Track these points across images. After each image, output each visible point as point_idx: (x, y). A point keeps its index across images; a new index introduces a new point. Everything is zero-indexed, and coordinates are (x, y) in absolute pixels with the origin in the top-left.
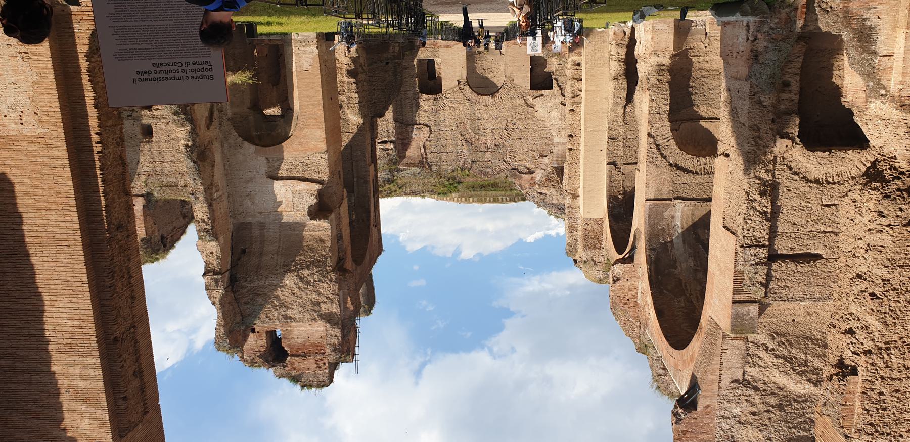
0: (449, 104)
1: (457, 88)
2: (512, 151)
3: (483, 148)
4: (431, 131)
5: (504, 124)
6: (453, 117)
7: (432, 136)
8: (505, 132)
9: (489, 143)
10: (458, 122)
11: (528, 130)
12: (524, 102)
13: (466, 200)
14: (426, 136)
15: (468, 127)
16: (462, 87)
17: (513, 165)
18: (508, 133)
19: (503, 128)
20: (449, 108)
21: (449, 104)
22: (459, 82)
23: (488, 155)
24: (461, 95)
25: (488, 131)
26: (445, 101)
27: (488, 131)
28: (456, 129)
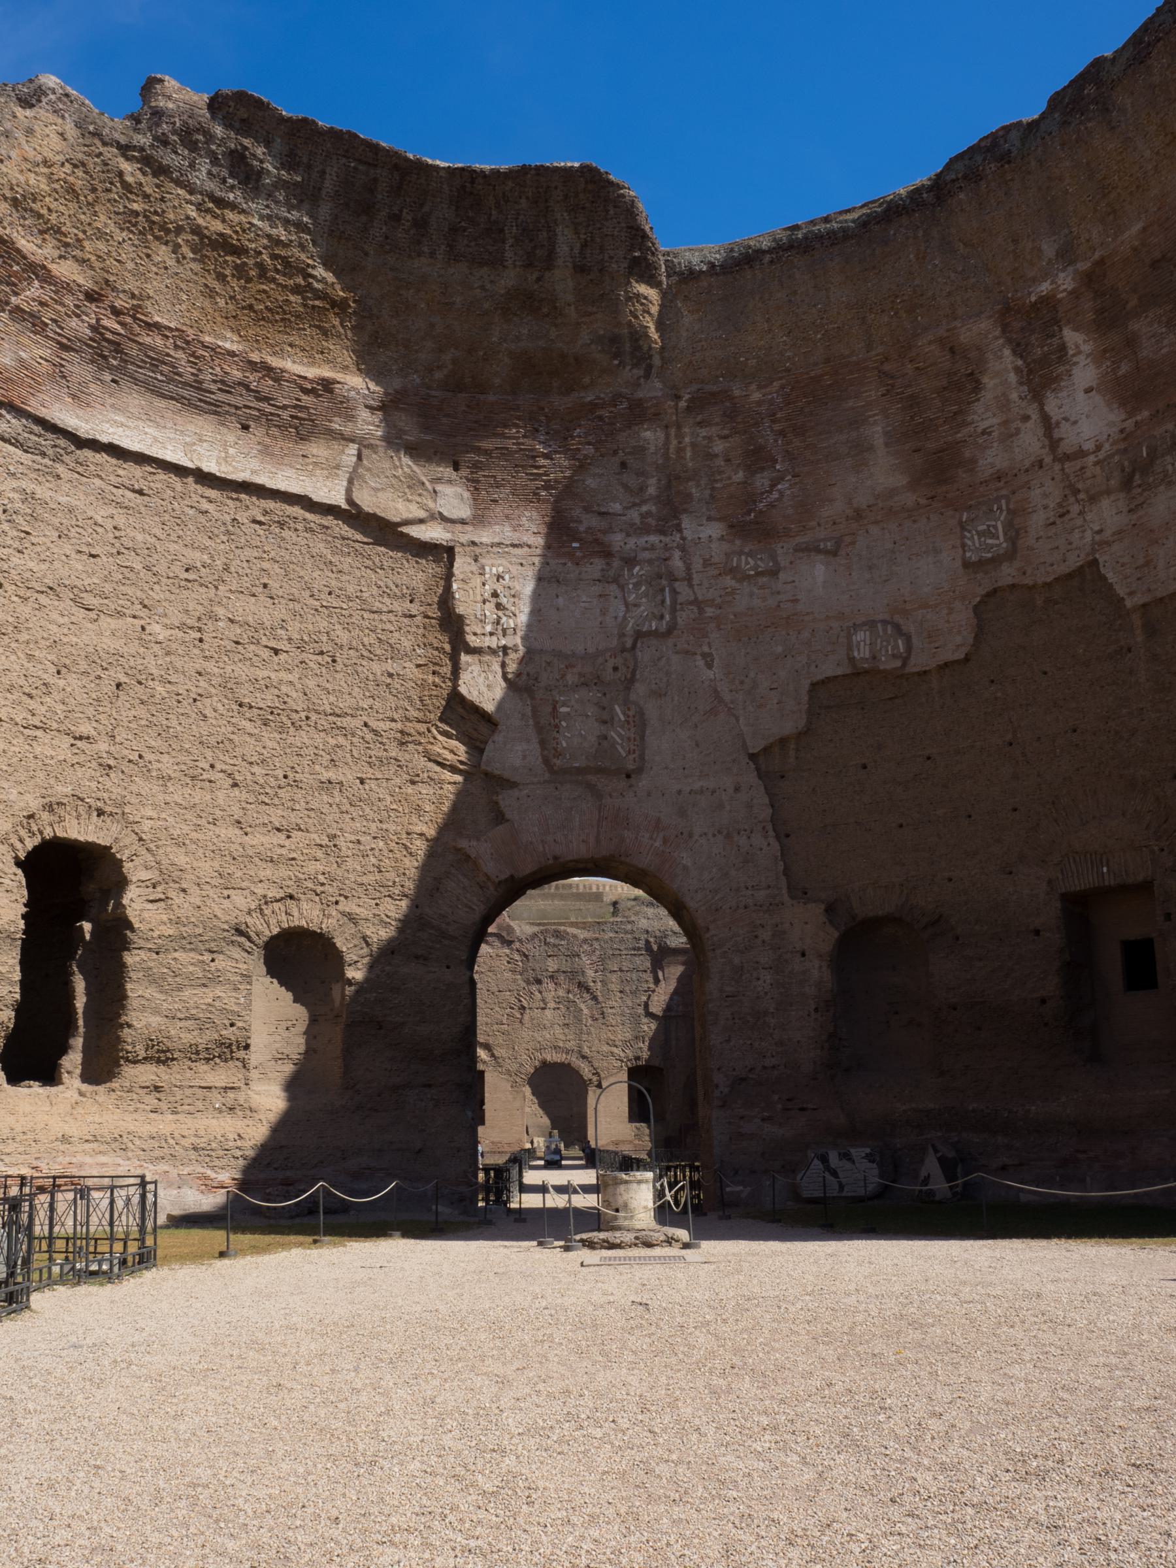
0: (615, 1050)
1: (602, 1075)
2: (513, 971)
3: (562, 977)
4: (646, 1005)
5: (526, 1017)
6: (610, 1028)
7: (644, 998)
8: (525, 1003)
9: (551, 986)
10: (601, 1021)
11: (488, 1005)
12: (495, 1052)
13: (591, 888)
14: (655, 998)
15: (586, 1011)
16: (595, 1078)
17: (512, 949)
18: (520, 1001)
19: (528, 1011)
20: (617, 1043)
21: (615, 1050)
22: (599, 1086)
23: (552, 965)
24: (596, 1064)
25: (552, 1005)
26: (622, 1055)
27: (552, 1005)
28: (605, 1010)
